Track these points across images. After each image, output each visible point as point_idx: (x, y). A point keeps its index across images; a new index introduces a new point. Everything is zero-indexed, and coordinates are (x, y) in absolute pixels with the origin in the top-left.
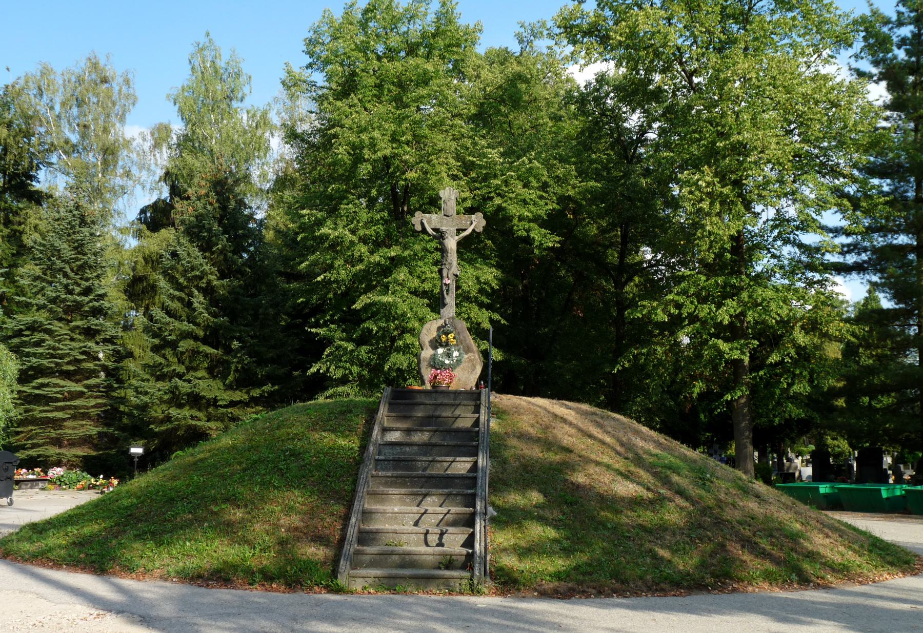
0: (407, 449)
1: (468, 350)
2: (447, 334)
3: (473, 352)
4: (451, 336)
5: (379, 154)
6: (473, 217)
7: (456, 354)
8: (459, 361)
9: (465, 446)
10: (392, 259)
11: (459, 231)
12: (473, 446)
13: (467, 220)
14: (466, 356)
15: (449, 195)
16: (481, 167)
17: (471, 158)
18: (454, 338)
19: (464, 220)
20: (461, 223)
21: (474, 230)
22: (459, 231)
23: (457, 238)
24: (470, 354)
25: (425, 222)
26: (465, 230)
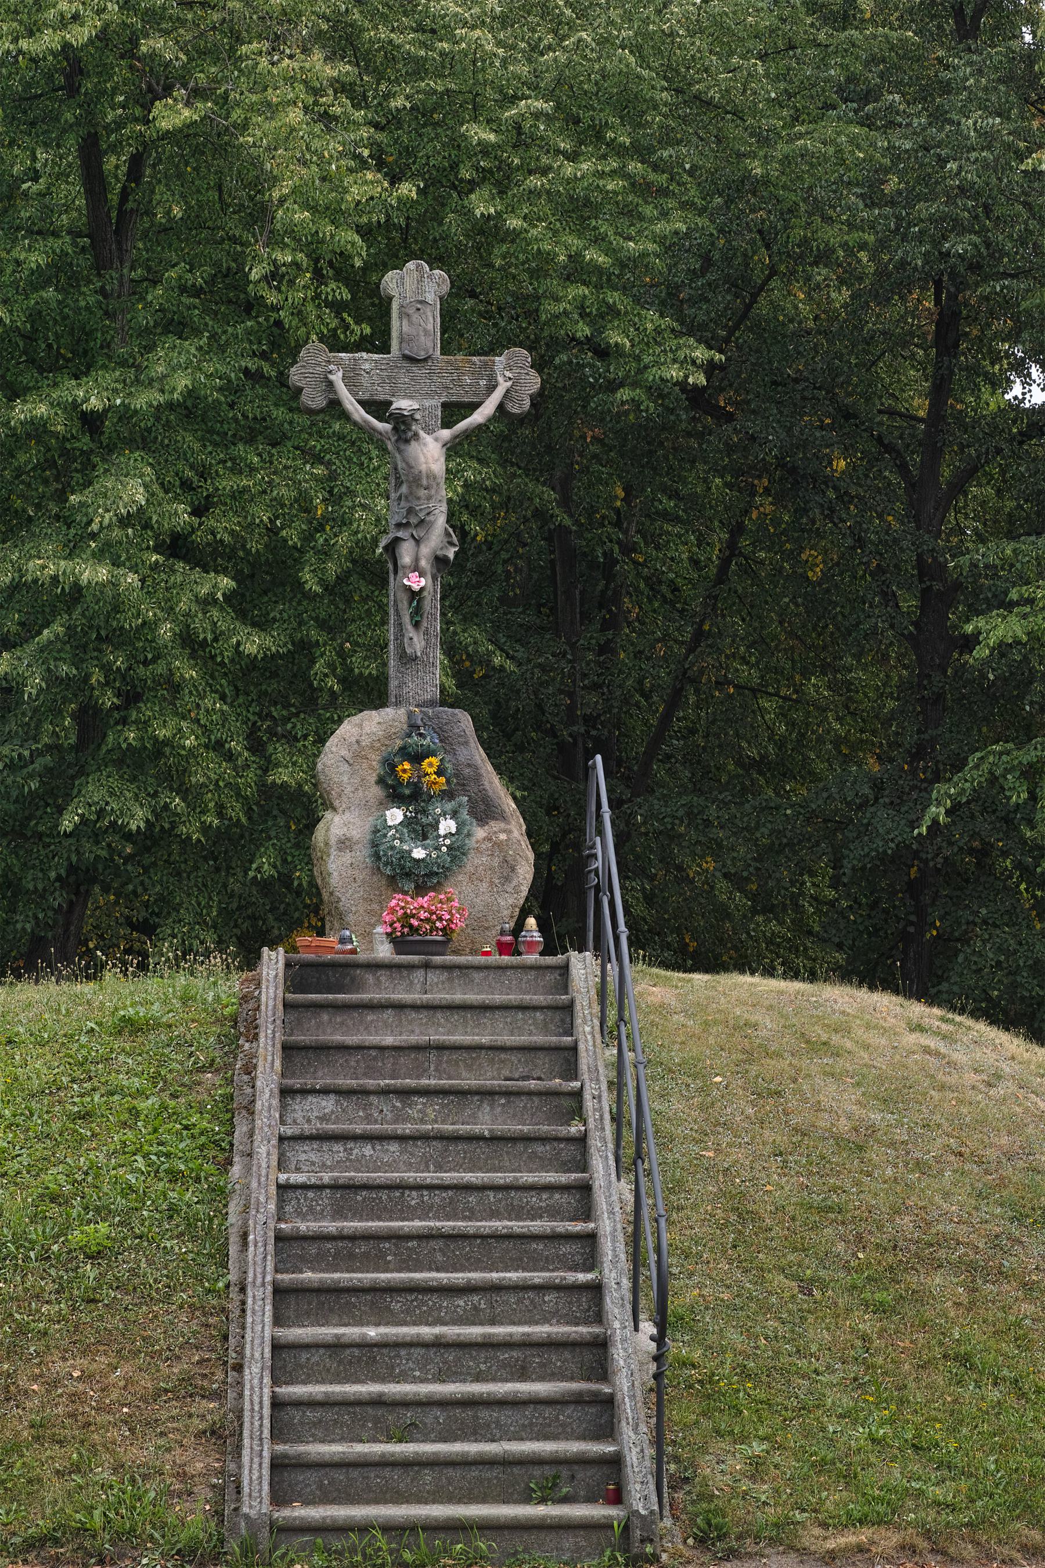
0: (368, 1150)
1: (484, 811)
2: (417, 758)
3: (502, 817)
4: (431, 764)
5: (49, 40)
6: (500, 361)
7: (447, 826)
8: (457, 851)
9: (543, 1139)
10: (91, 422)
11: (453, 412)
12: (570, 1140)
13: (476, 374)
14: (480, 833)
15: (420, 290)
16: (419, 69)
17: (384, 33)
18: (439, 773)
19: (461, 373)
20: (458, 382)
21: (501, 407)
22: (453, 412)
23: (446, 434)
24: (495, 825)
25: (337, 378)
26: (474, 406)
